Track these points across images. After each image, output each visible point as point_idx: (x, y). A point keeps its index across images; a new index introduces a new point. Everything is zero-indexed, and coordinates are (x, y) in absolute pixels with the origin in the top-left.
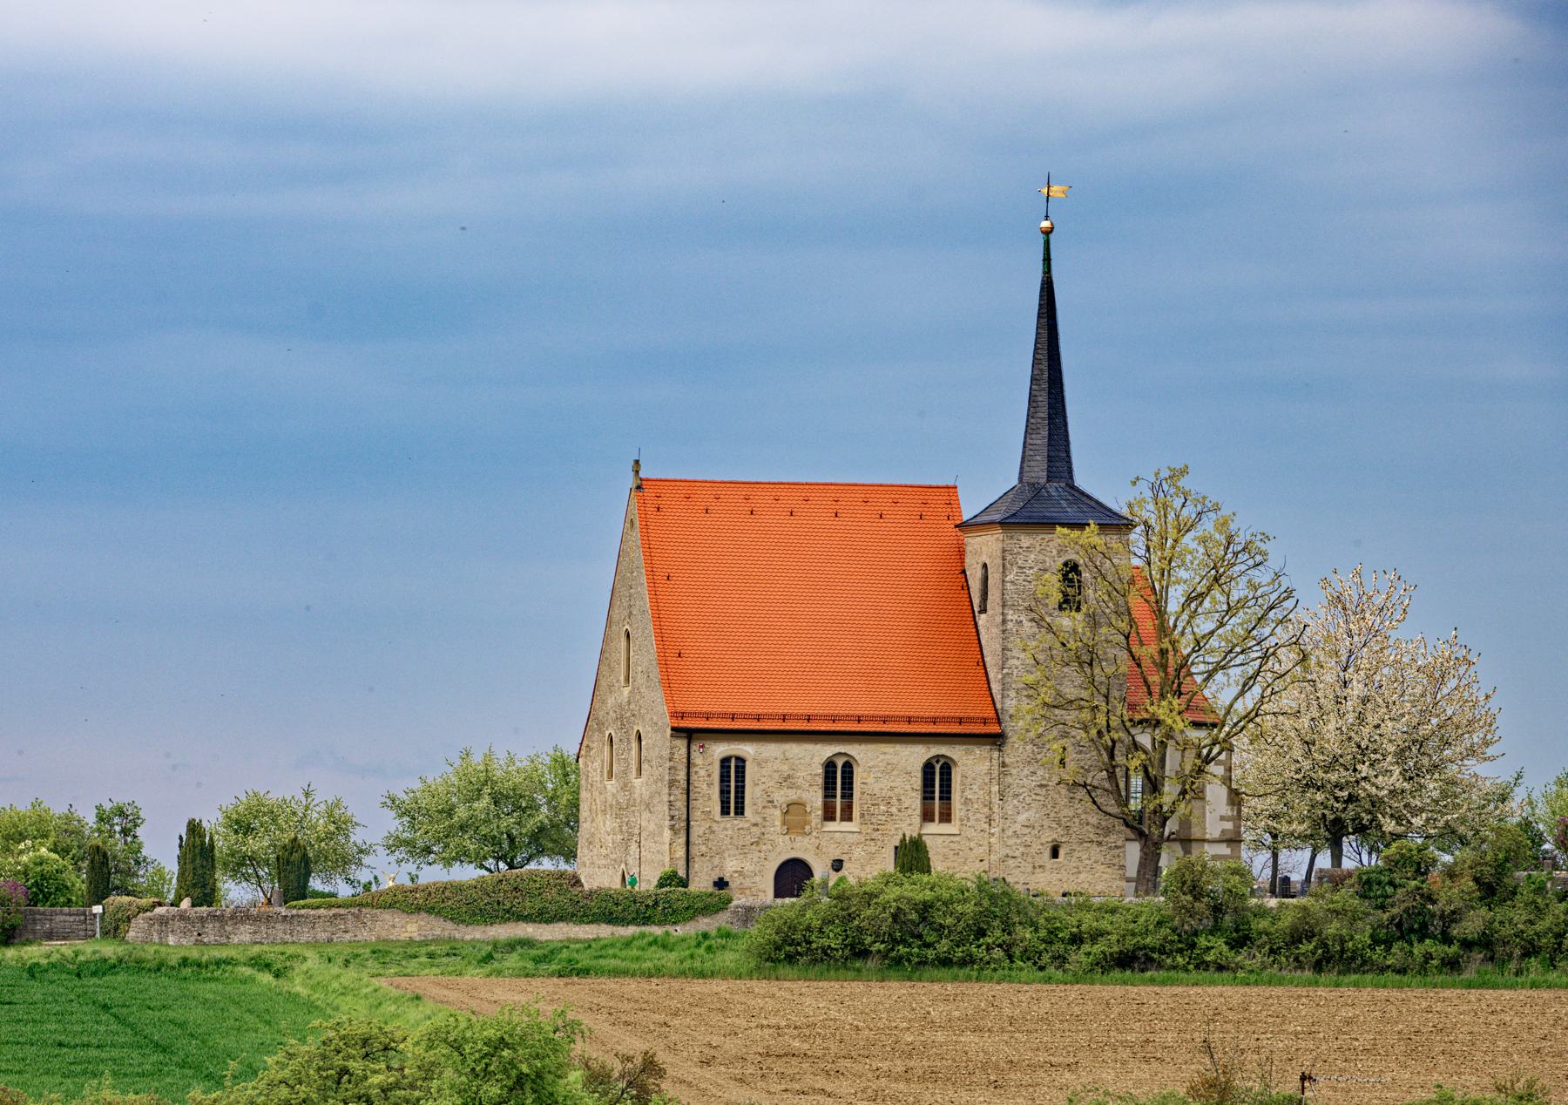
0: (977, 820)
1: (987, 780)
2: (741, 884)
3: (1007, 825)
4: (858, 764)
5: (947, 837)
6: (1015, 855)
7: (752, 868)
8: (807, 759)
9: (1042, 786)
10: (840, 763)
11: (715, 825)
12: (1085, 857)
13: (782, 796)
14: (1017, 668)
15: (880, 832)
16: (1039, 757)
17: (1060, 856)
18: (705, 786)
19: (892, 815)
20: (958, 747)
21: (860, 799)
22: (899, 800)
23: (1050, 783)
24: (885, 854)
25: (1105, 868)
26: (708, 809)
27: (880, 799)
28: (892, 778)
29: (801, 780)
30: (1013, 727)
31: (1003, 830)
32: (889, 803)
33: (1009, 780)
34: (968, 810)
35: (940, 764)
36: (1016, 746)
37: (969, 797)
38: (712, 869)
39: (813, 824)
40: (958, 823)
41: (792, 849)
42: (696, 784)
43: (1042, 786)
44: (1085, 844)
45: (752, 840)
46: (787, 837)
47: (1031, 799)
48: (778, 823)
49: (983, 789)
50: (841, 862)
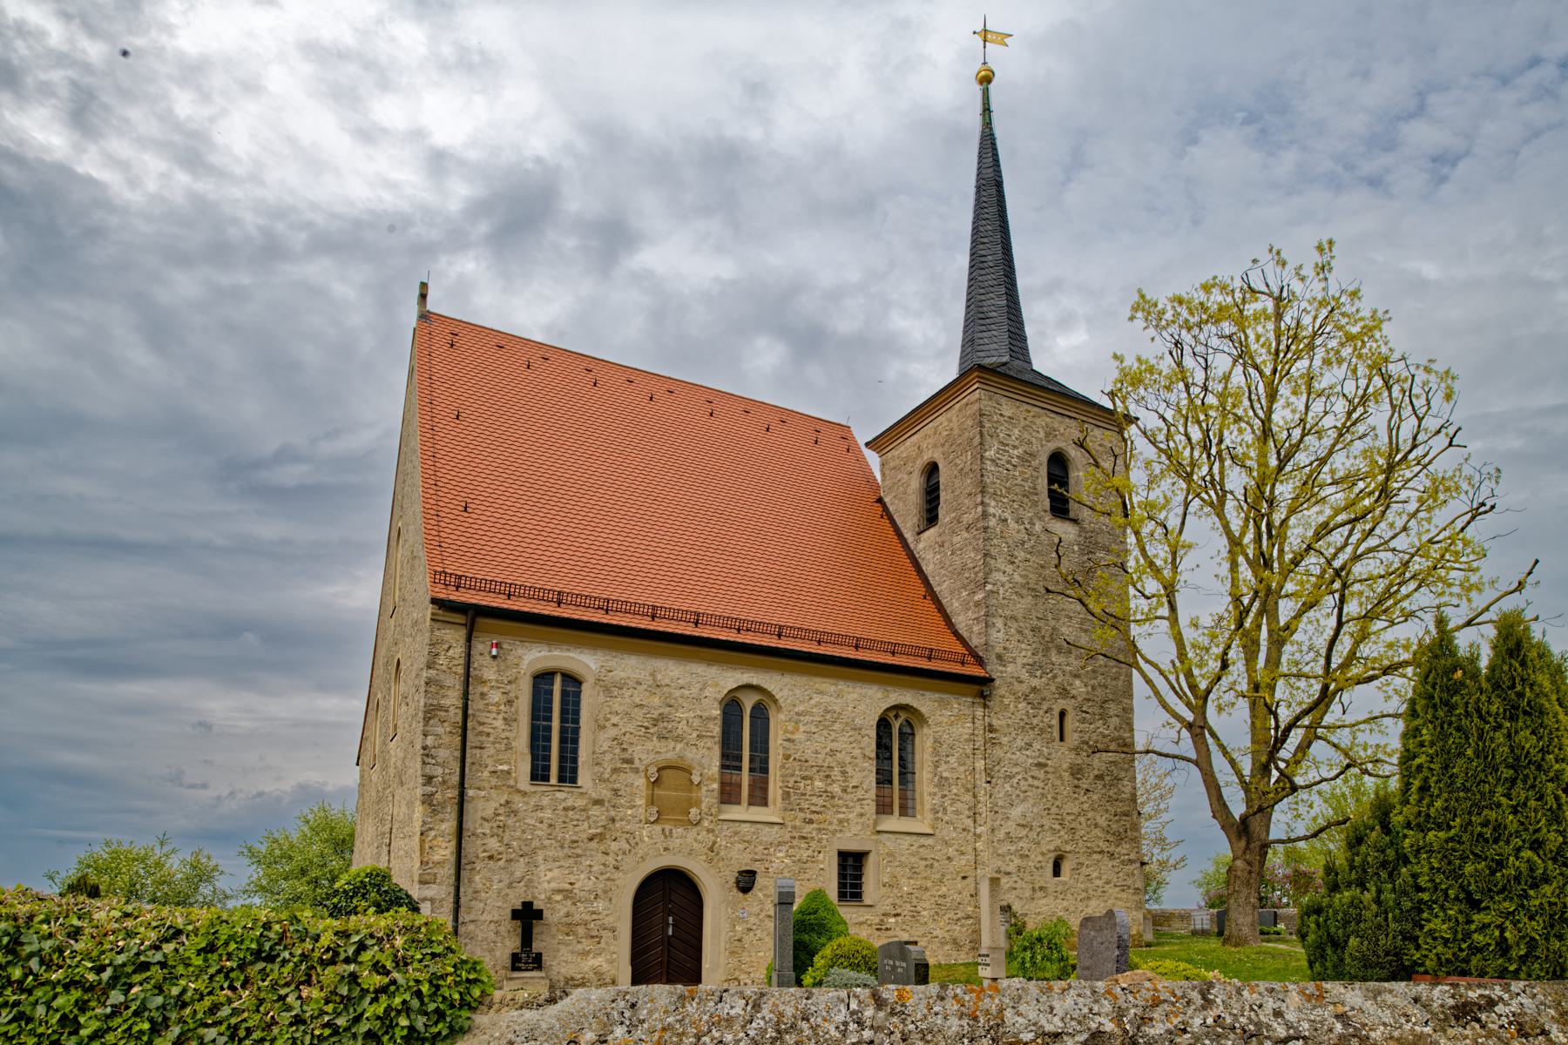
0: (957, 812)
1: (969, 751)
2: (568, 915)
3: (998, 823)
4: (779, 709)
5: (915, 838)
7: (590, 884)
9: (1040, 765)
10: (748, 702)
11: (517, 798)
12: (1095, 875)
13: (648, 753)
14: (1003, 586)
15: (815, 825)
16: (1035, 721)
17: (1062, 872)
18: (499, 723)
19: (833, 797)
21: (783, 767)
22: (844, 773)
23: (1049, 762)
24: (822, 862)
25: (1118, 893)
26: (505, 768)
27: (815, 769)
29: (683, 725)
30: (1002, 672)
32: (828, 776)
33: (998, 752)
34: (944, 796)
35: (900, 720)
37: (945, 774)
38: (510, 886)
39: (703, 806)
40: (929, 816)
41: (666, 849)
42: (482, 717)
43: (1040, 765)
44: (1096, 856)
45: (592, 831)
46: (658, 828)
47: (1026, 783)
48: (640, 802)
49: (964, 764)
50: (753, 873)
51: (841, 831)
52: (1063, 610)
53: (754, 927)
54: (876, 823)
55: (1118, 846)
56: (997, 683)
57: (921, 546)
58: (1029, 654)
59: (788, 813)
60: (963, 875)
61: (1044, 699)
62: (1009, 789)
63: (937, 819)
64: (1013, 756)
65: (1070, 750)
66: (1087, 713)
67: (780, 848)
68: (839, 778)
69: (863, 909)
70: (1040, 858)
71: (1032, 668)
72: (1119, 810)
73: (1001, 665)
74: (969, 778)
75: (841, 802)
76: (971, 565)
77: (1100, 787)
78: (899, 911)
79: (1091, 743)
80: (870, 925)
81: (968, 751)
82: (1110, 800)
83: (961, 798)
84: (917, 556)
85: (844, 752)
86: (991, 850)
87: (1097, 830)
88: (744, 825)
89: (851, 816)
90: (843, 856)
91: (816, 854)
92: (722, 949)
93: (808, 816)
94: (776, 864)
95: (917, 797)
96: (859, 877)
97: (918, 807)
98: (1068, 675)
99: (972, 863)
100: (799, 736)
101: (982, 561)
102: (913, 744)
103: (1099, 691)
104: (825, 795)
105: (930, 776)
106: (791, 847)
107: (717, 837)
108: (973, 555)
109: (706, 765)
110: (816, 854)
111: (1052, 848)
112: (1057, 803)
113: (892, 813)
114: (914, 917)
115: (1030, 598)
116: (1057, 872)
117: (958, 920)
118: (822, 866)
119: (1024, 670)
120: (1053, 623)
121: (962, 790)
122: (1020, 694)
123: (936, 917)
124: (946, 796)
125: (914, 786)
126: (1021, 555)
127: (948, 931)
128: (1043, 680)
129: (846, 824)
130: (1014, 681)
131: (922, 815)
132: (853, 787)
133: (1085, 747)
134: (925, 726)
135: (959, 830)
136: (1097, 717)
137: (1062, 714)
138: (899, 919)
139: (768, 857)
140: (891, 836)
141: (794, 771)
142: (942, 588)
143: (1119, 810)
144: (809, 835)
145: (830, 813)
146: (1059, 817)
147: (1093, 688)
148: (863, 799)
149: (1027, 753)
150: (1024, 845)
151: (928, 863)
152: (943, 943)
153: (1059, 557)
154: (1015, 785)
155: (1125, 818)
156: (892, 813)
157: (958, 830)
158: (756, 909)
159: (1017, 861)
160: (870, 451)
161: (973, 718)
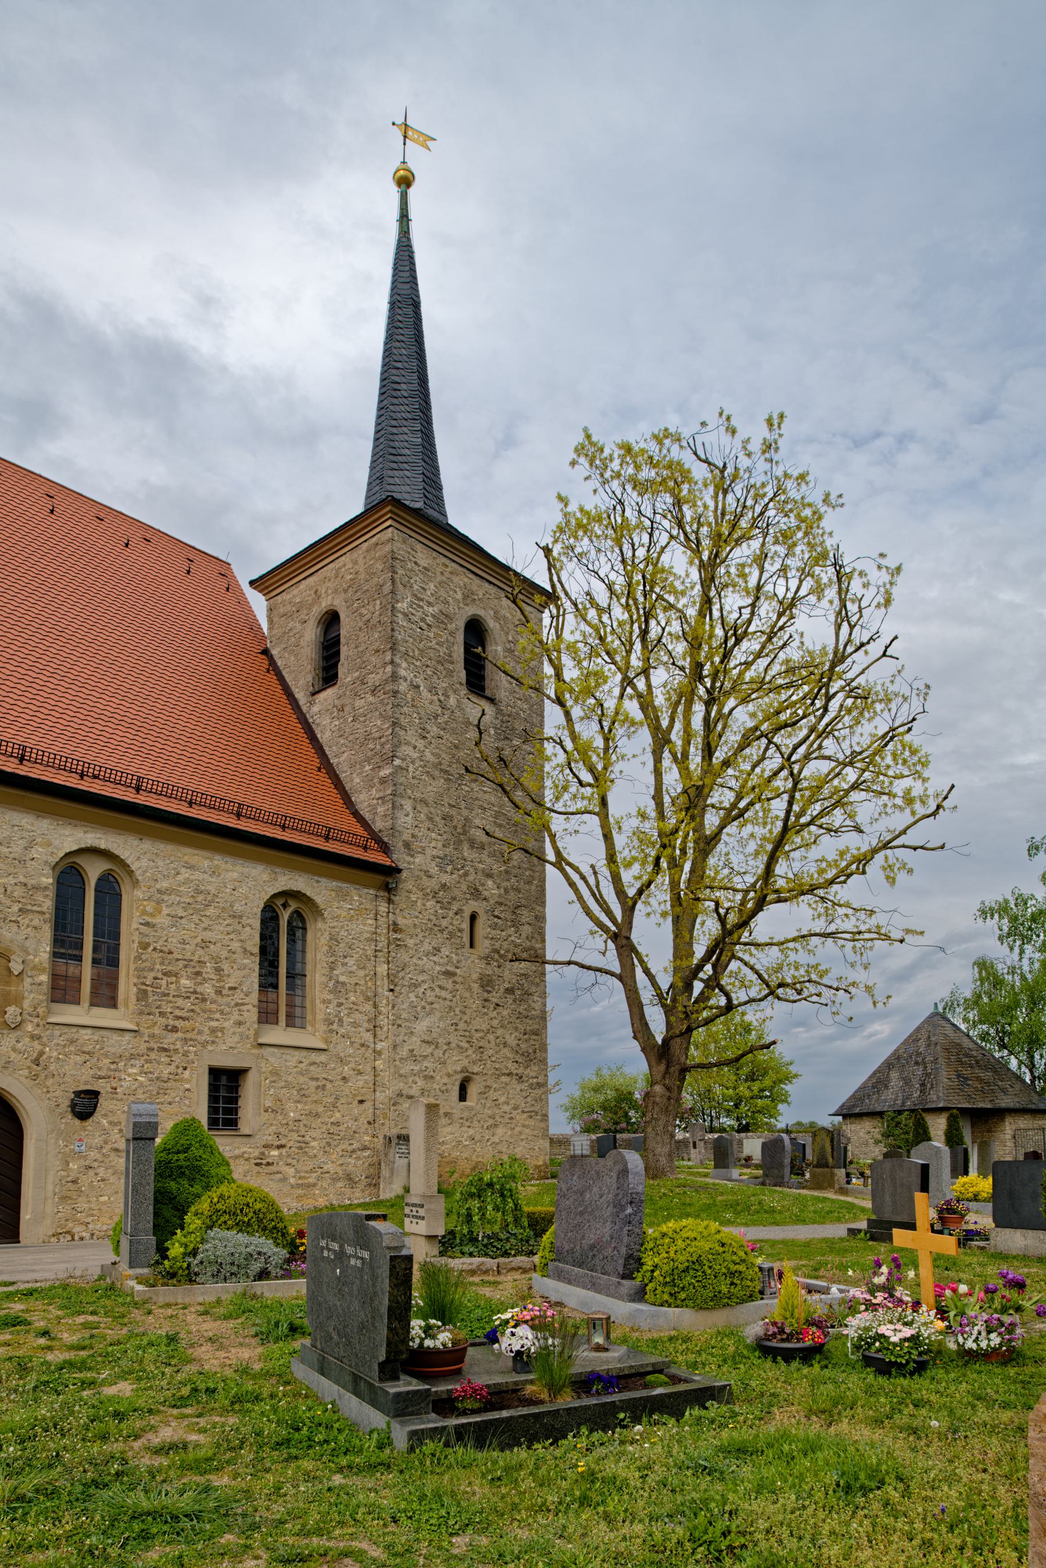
0: (355, 1024)
3: (401, 1038)
4: (136, 883)
5: (304, 1053)
6: (412, 1093)
8: (17, 849)
9: (448, 974)
10: (93, 871)
14: (413, 762)
15: (180, 1035)
16: (444, 923)
17: (468, 1096)
19: (204, 1000)
20: (324, 881)
21: (138, 958)
22: (218, 970)
23: (458, 971)
24: (188, 1081)
27: (181, 964)
28: (206, 922)
30: (409, 863)
31: (395, 1047)
32: (198, 973)
33: (403, 956)
34: (340, 1005)
35: (290, 910)
36: (413, 897)
37: (342, 979)
39: (26, 1004)
40: (322, 1027)
43: (448, 974)
44: (504, 1079)
47: (433, 994)
49: (364, 968)
50: (95, 1094)
51: (213, 1042)
52: (477, 799)
53: (95, 1164)
54: (257, 1035)
55: (526, 1068)
56: (404, 874)
57: (315, 709)
58: (440, 845)
59: (145, 1018)
60: (360, 1098)
61: (454, 899)
62: (414, 999)
63: (331, 1031)
64: (420, 962)
65: (481, 958)
66: (499, 918)
67: (133, 1062)
68: (212, 976)
69: (239, 1139)
70: (445, 1080)
71: (443, 861)
72: (528, 1028)
73: (409, 855)
74: (370, 984)
75: (214, 1006)
76: (377, 735)
77: (510, 1001)
78: (283, 1142)
79: (502, 952)
80: (246, 1160)
81: (369, 952)
82: (520, 1016)
83: (360, 1008)
84: (311, 720)
85: (219, 945)
86: (392, 1070)
87: (506, 1050)
88: (83, 1031)
89: (226, 1024)
90: (215, 1073)
91: (180, 1070)
92: (50, 1194)
93: (171, 1022)
94: (127, 1083)
95: (308, 1005)
96: (235, 1100)
97: (309, 1017)
98: (480, 873)
99: (371, 1085)
100: (162, 920)
101: (390, 731)
102: (304, 941)
103: (512, 895)
104: (193, 997)
105: (324, 979)
106: (147, 1061)
107: (44, 1045)
108: (379, 723)
109: (31, 950)
110: (180, 1070)
111: (459, 1069)
112: (466, 1018)
113: (277, 1023)
114: (301, 1148)
115: (442, 781)
116: (463, 1097)
117: (353, 1151)
118: (187, 1086)
119: (433, 864)
120: (465, 812)
121: (361, 999)
122: (428, 891)
123: (328, 1149)
124: (342, 1004)
125: (304, 991)
126: (434, 730)
127: (341, 1165)
128: (454, 876)
129: (220, 1034)
130: (422, 874)
131: (313, 1026)
132: (231, 988)
133: (496, 956)
134: (320, 919)
135: (356, 1045)
136: (509, 924)
137: (473, 917)
138: (284, 1151)
139: (117, 1074)
140: (276, 1050)
141: (154, 964)
142: (341, 760)
143: (528, 1028)
144: (172, 1047)
145: (199, 1020)
146: (467, 1034)
147: (506, 890)
148: (243, 1004)
149: (435, 959)
150: (428, 1065)
151: (320, 1084)
152: (335, 1180)
153: (481, 733)
154: (420, 995)
155: (534, 1037)
156: (277, 1023)
157: (356, 1045)
158: (98, 1141)
159: (421, 1083)
160: (255, 592)
161: (376, 914)
